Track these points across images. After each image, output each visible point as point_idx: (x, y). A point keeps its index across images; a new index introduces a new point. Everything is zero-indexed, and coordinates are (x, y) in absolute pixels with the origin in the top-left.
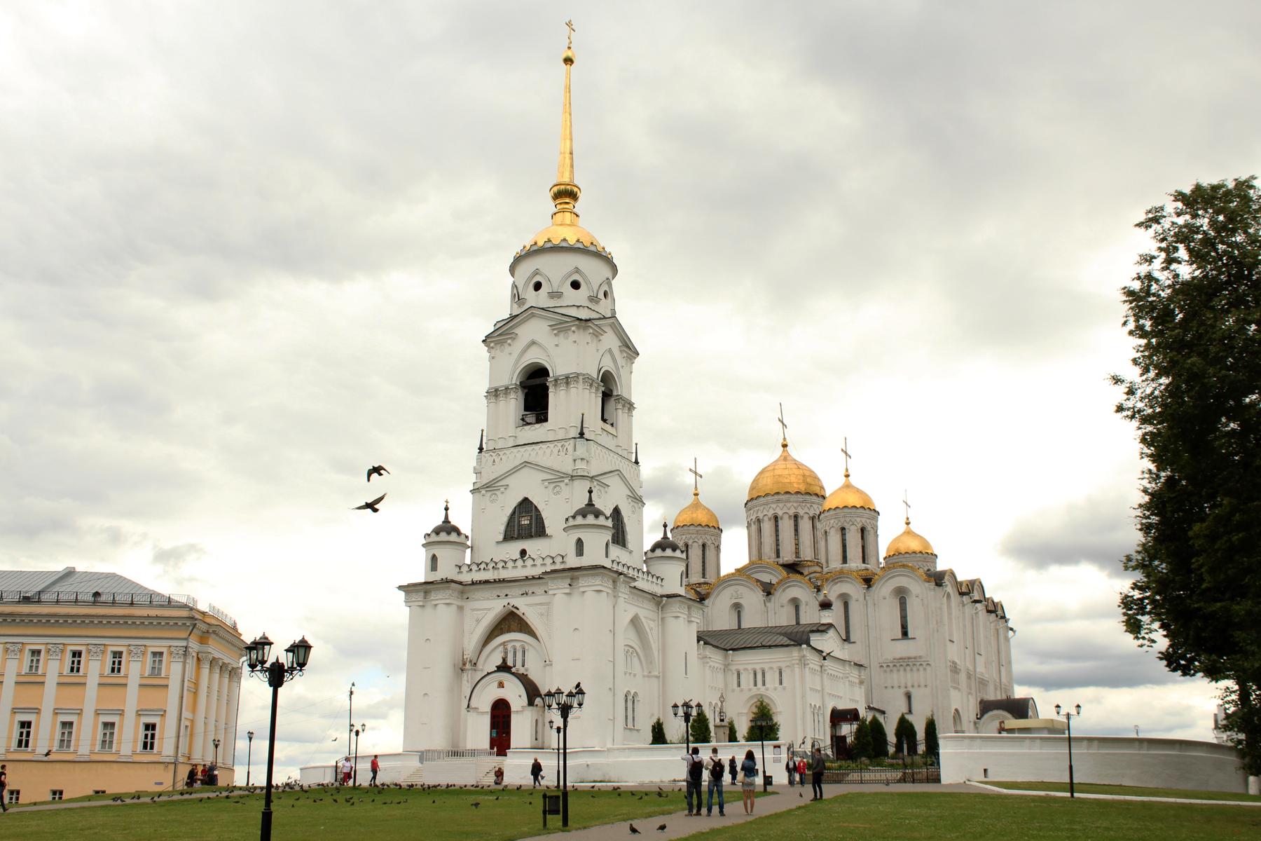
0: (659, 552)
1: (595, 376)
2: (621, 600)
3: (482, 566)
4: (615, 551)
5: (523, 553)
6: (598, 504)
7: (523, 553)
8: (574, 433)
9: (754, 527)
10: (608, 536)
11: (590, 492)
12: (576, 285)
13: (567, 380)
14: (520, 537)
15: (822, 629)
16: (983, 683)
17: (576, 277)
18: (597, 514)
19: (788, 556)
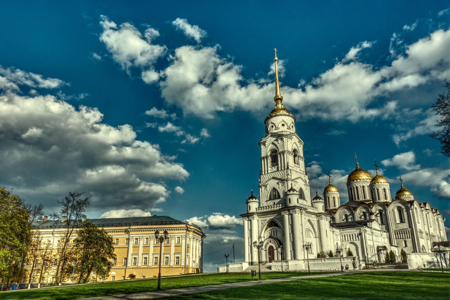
0: (315, 201)
1: (291, 150)
2: (303, 215)
3: (263, 208)
4: (301, 201)
5: (274, 203)
6: (294, 188)
7: (274, 203)
8: (286, 167)
9: (350, 191)
10: (297, 197)
11: (291, 184)
12: (283, 125)
13: (283, 153)
14: (273, 199)
15: (371, 221)
16: (433, 236)
17: (283, 123)
18: (294, 190)
19: (361, 199)
